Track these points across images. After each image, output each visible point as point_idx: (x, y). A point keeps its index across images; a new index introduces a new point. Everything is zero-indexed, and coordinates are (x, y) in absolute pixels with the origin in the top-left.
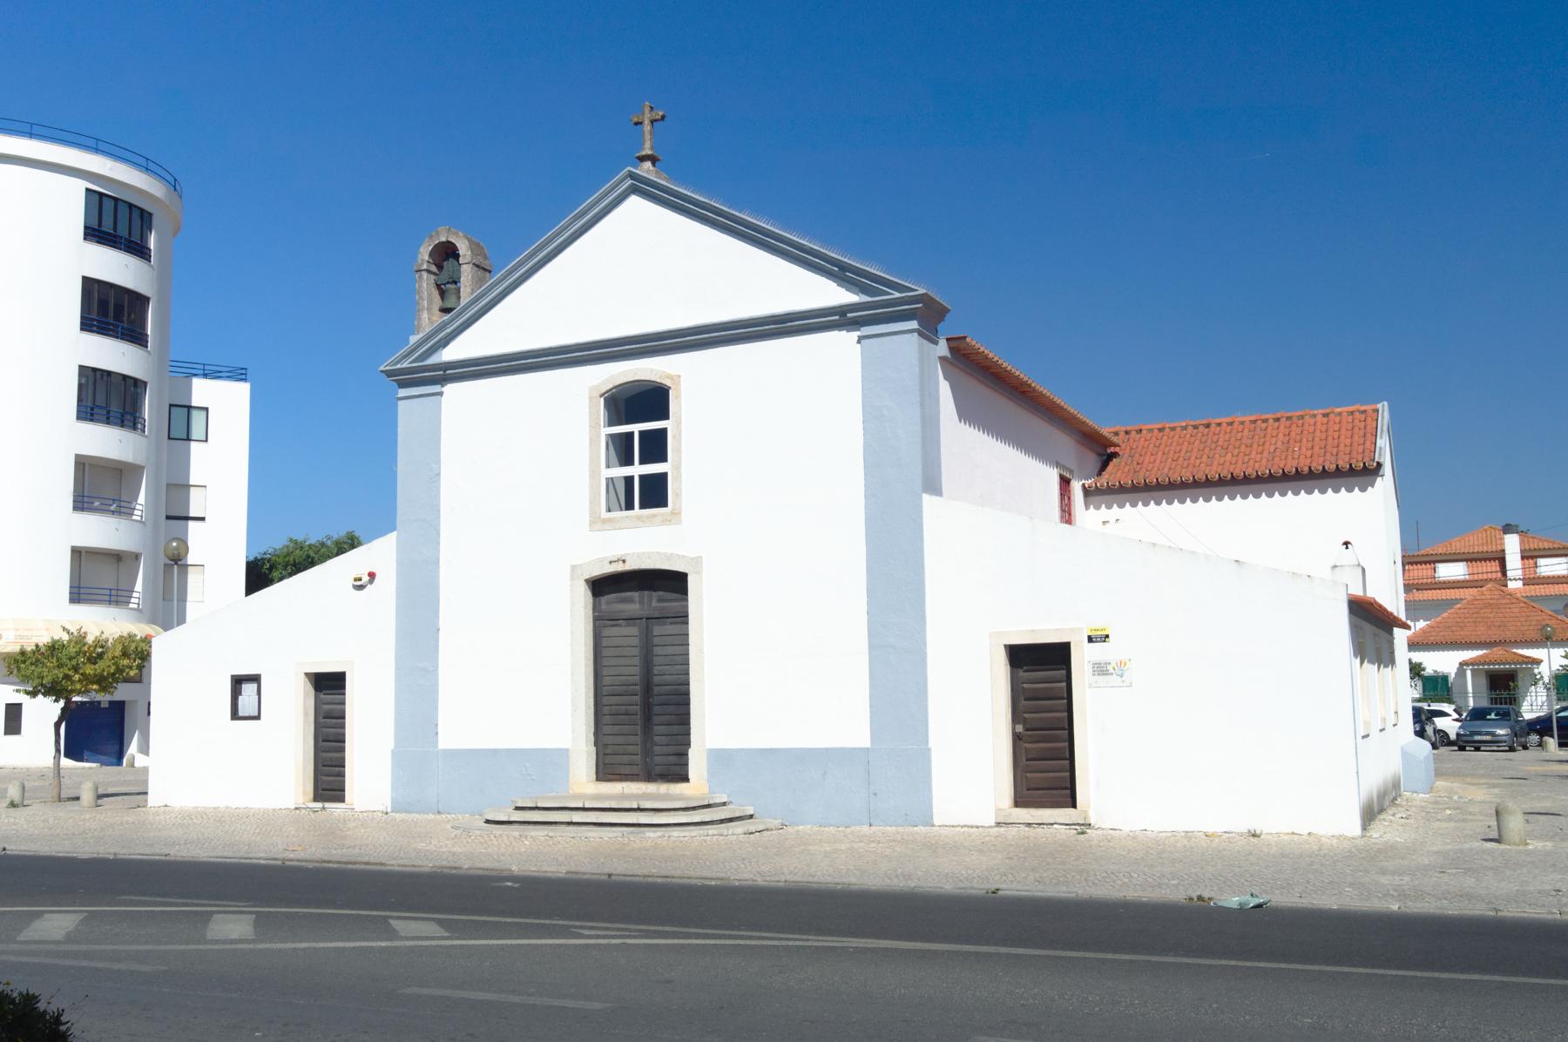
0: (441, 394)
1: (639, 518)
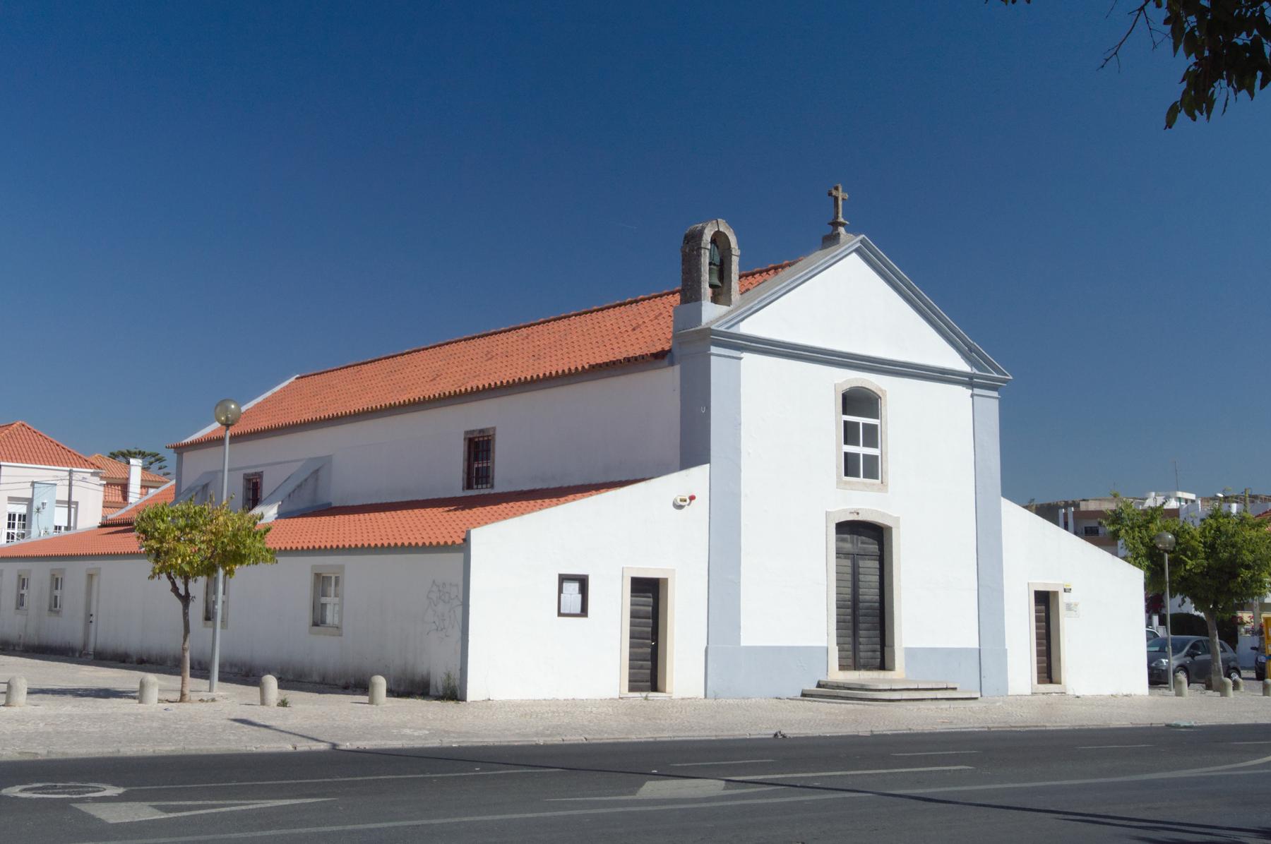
0: (740, 359)
1: (865, 484)
